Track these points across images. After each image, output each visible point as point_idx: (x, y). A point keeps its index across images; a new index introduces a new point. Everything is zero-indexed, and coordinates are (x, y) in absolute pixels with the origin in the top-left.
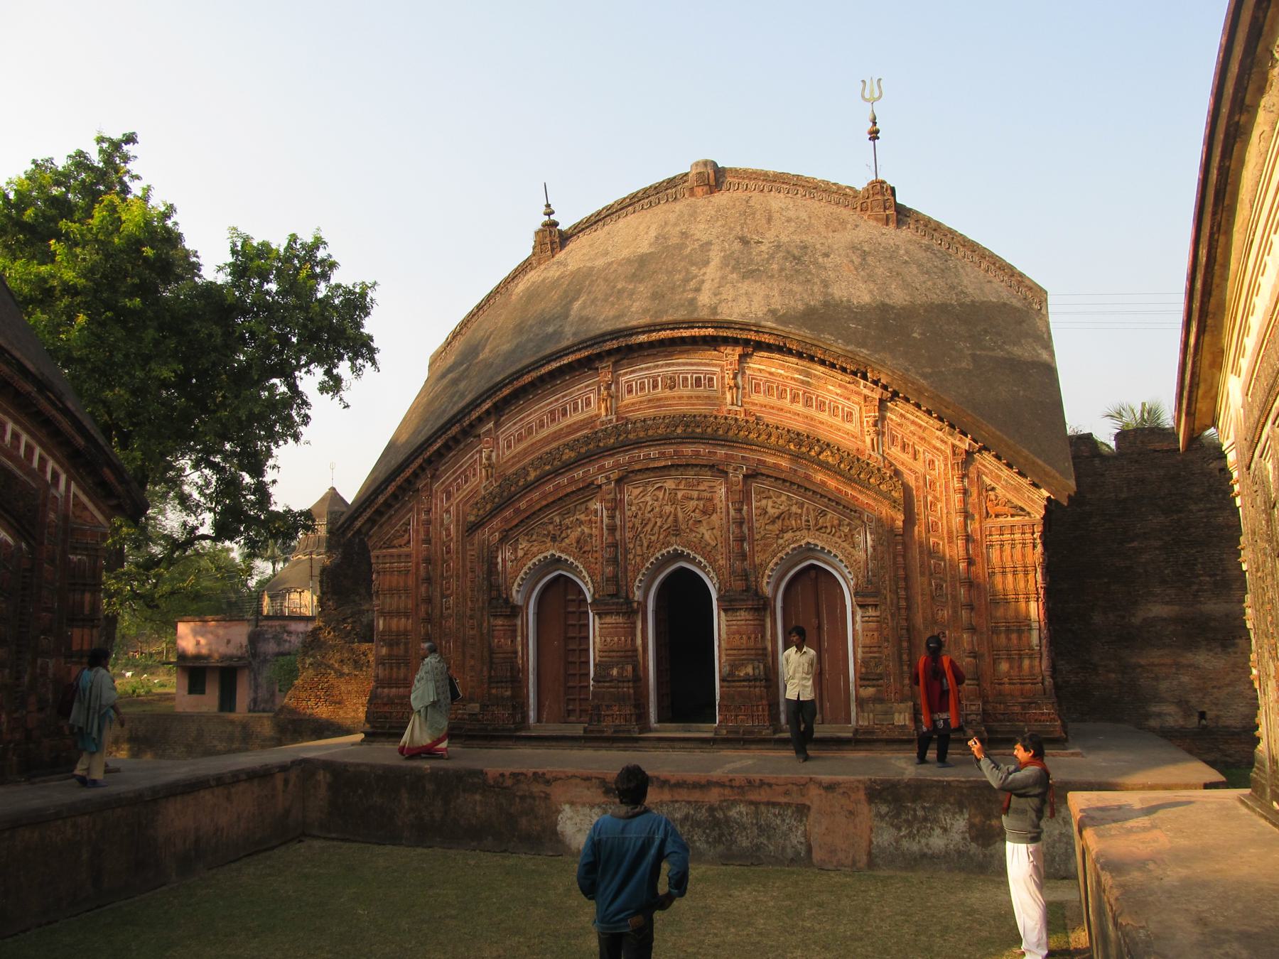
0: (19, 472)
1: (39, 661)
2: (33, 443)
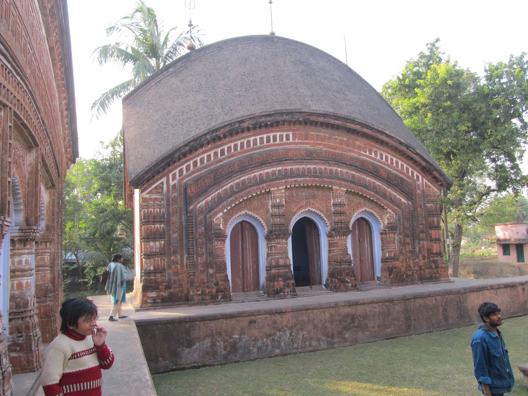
0: (405, 178)
1: (421, 242)
2: (408, 167)
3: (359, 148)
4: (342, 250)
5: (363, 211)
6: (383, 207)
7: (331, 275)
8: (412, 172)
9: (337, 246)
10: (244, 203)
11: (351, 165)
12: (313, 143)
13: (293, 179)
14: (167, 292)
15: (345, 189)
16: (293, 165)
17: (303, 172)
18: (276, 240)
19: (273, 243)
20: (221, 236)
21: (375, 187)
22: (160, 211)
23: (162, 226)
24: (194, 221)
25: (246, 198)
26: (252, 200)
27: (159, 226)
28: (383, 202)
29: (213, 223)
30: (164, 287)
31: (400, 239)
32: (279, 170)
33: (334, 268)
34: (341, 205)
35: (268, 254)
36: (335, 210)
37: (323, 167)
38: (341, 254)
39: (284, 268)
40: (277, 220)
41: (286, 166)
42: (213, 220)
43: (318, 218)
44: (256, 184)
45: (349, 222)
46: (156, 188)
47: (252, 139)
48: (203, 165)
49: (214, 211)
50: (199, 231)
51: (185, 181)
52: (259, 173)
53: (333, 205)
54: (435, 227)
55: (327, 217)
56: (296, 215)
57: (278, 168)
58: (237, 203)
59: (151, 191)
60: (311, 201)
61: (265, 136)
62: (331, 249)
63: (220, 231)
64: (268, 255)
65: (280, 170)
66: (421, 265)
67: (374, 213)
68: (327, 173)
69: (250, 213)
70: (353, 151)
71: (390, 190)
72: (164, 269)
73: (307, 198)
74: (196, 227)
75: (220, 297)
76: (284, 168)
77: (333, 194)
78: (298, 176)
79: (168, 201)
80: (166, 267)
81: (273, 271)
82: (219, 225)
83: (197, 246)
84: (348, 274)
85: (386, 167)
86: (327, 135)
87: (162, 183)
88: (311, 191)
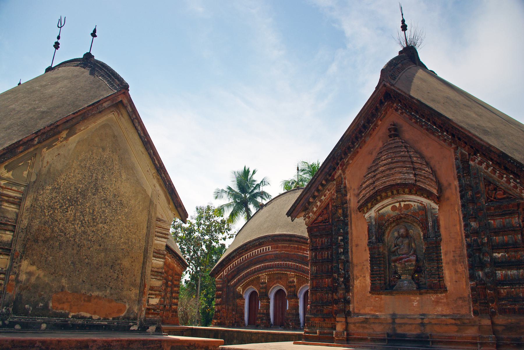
17: (273, 266)
20: (241, 297)
57: (262, 265)
70: (300, 252)
73: (277, 279)
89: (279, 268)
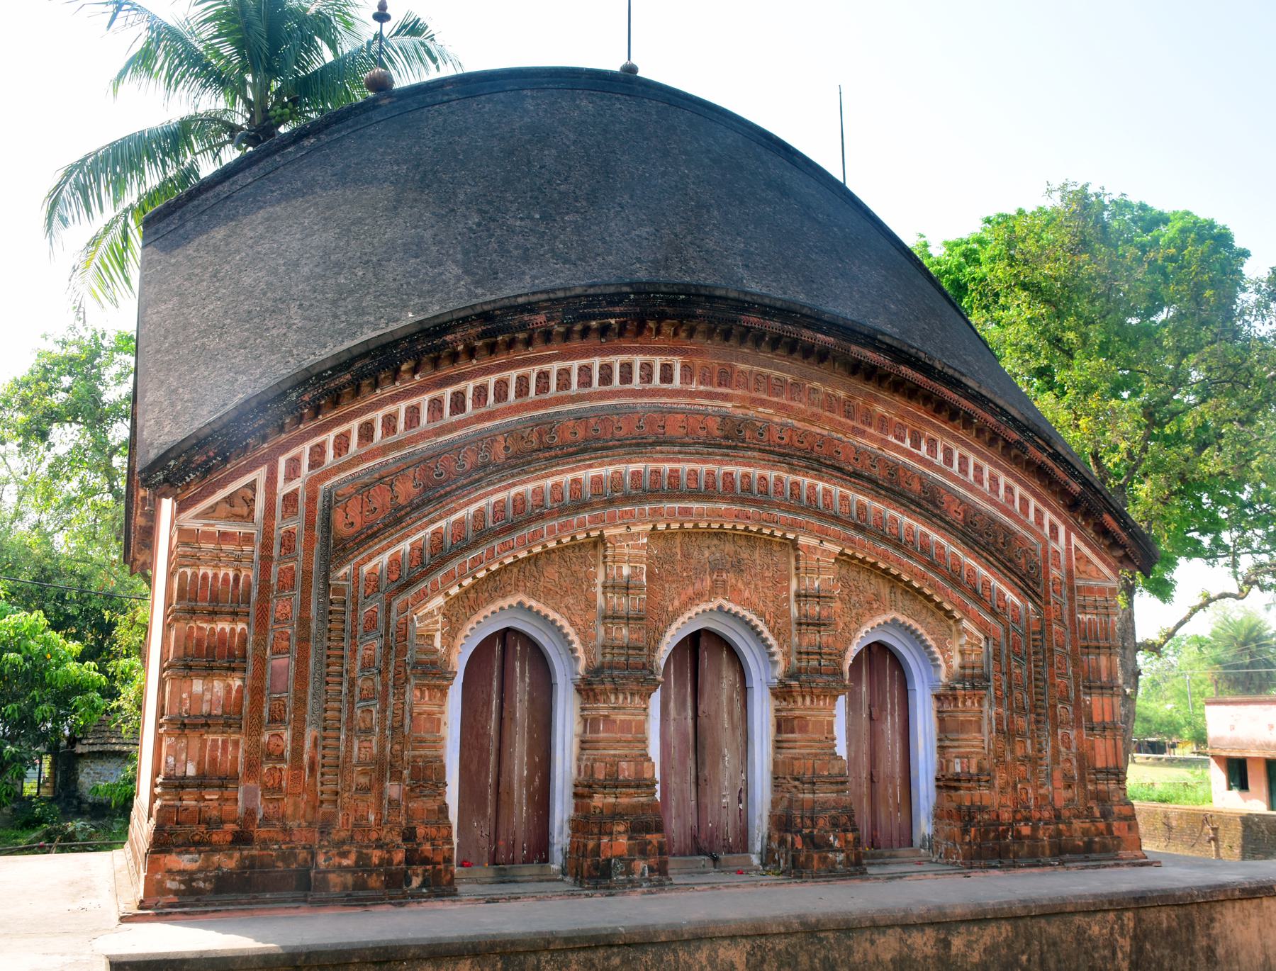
0: (1016, 527)
1: (1060, 731)
3: (884, 424)
4: (820, 741)
5: (885, 623)
6: (949, 614)
7: (782, 823)
8: (1037, 510)
9: (803, 729)
10: (515, 570)
11: (856, 475)
12: (742, 398)
13: (677, 505)
14: (237, 855)
15: (837, 549)
16: (679, 461)
18: (613, 698)
19: (602, 709)
21: (926, 549)
22: (237, 578)
23: (240, 626)
24: (348, 618)
25: (523, 554)
26: (541, 563)
27: (227, 627)
28: (949, 598)
29: (410, 628)
30: (229, 838)
31: (999, 719)
32: (633, 473)
33: (790, 801)
34: (819, 597)
35: (583, 742)
36: (803, 612)
37: (771, 475)
38: (816, 755)
39: (632, 790)
40: (624, 633)
41: (656, 461)
42: (412, 620)
43: (743, 633)
44: (563, 510)
45: (841, 655)
46: (229, 500)
47: (555, 367)
48: (391, 439)
49: (416, 590)
50: (361, 650)
51: (328, 483)
52: (569, 477)
53: (798, 596)
54: (1102, 688)
55: (777, 634)
56: (681, 620)
57: (633, 467)
58: (494, 567)
59: (213, 508)
60: (730, 578)
61: (596, 362)
62: (785, 736)
63: (433, 657)
64: (584, 744)
65: (638, 472)
66: (1059, 803)
67: (921, 631)
68: (782, 493)
69: (533, 603)
70: (862, 433)
71: (973, 563)
72: (235, 778)
73: (716, 568)
74: (354, 637)
75: (416, 882)
76: (652, 466)
77: (797, 559)
78: (695, 495)
79: (266, 546)
80: (240, 769)
81: (598, 800)
82: (431, 637)
83: (352, 704)
84: (835, 824)
85: (961, 490)
86: (789, 378)
87: (252, 486)
88: (729, 548)
89: (754, 503)
